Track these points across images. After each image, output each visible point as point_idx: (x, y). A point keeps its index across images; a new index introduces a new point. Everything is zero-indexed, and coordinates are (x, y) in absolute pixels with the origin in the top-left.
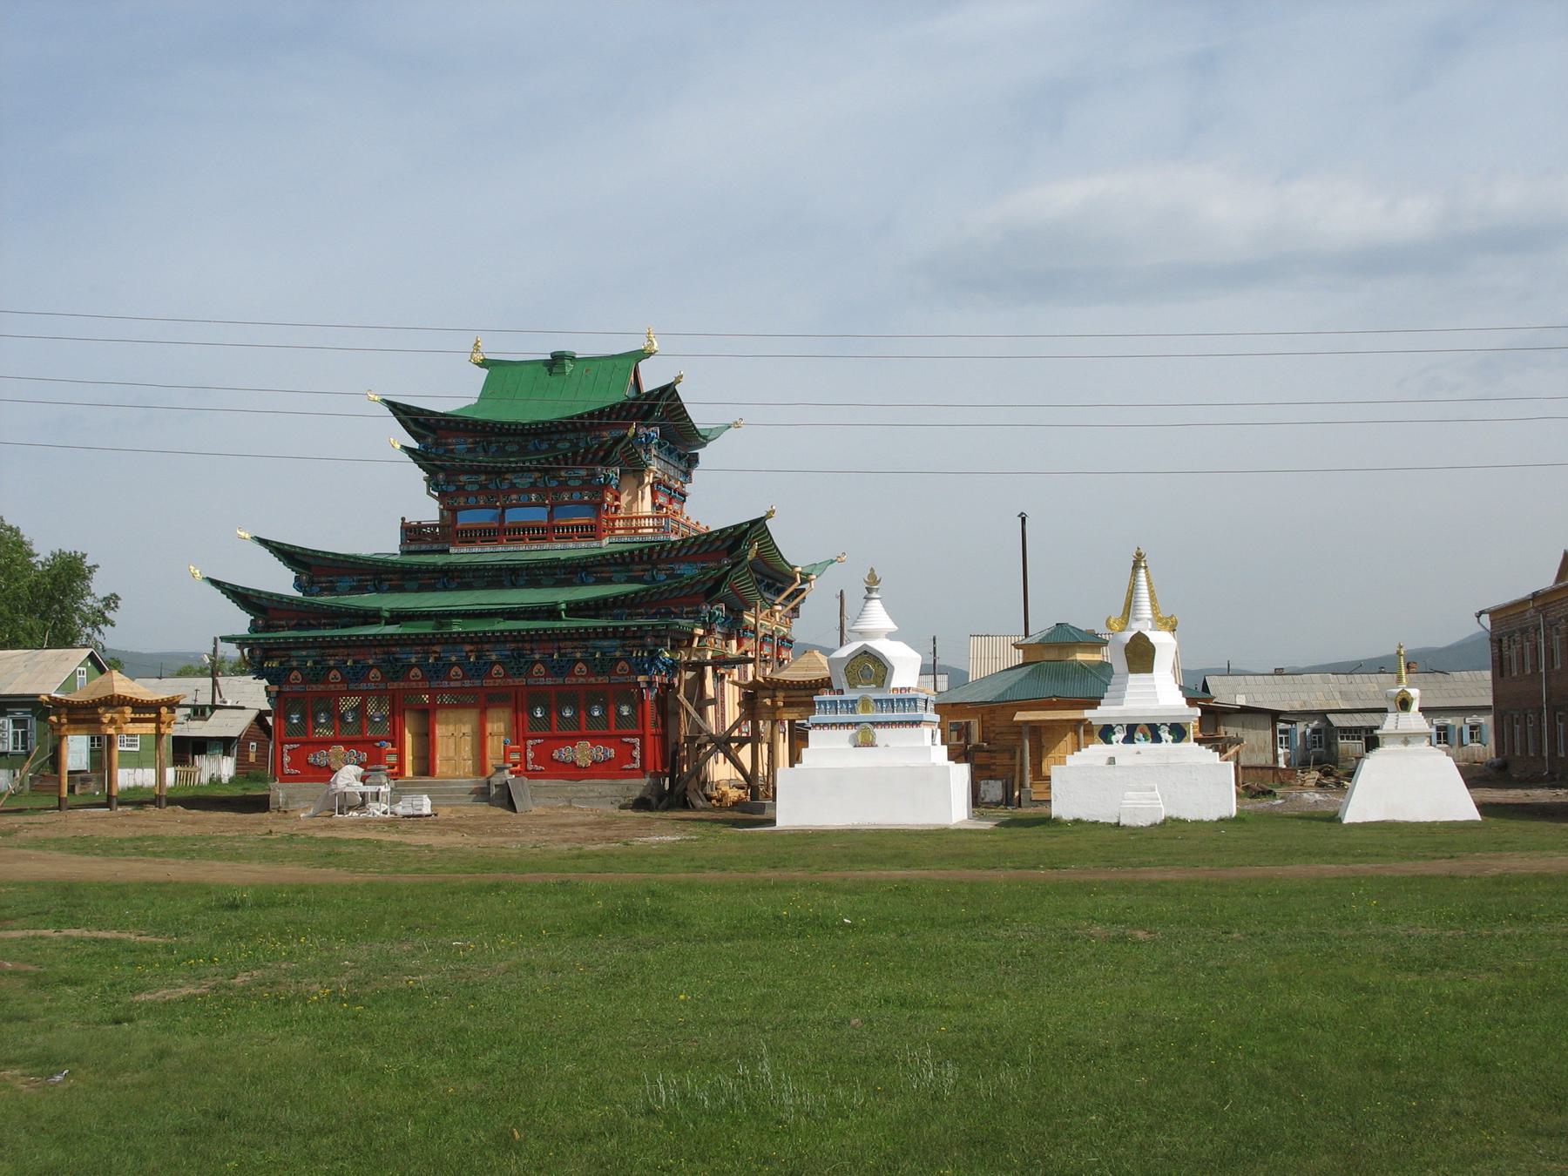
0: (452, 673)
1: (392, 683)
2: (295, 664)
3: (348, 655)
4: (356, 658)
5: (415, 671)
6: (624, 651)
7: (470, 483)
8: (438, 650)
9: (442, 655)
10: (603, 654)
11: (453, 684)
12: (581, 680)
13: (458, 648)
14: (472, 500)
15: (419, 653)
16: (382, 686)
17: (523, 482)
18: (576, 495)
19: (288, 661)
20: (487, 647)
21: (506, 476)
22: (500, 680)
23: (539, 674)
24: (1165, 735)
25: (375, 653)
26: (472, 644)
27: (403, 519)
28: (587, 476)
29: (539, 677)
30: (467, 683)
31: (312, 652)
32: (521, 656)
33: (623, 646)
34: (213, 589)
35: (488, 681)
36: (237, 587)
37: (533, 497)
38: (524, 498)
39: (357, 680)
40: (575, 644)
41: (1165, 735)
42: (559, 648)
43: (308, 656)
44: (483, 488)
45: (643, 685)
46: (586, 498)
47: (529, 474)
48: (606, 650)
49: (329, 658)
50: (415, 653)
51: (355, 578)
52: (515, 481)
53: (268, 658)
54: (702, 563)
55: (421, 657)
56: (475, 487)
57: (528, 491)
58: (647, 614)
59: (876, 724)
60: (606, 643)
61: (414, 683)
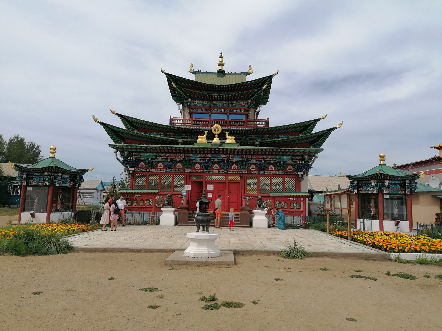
0: (214, 167)
1: (187, 170)
2: (142, 159)
4: (172, 158)
5: (198, 165)
6: (293, 161)
9: (211, 159)
10: (283, 162)
11: (215, 171)
12: (272, 172)
14: (200, 110)
15: (201, 157)
16: (182, 171)
17: (219, 104)
19: (139, 158)
20: (232, 156)
21: (213, 102)
22: (236, 171)
23: (253, 169)
26: (225, 154)
27: (171, 116)
28: (243, 104)
29: (253, 170)
30: (221, 172)
31: (152, 154)
32: (247, 161)
33: (292, 159)
34: (102, 127)
35: (230, 171)
36: (114, 127)
37: (223, 110)
38: (219, 111)
39: (171, 168)
40: (271, 157)
42: (264, 158)
43: (149, 156)
44: (204, 106)
46: (242, 112)
48: (284, 160)
49: (159, 157)
50: (199, 157)
51: (156, 134)
52: (216, 104)
53: (129, 156)
55: (202, 159)
57: (221, 108)
60: (284, 157)
61: (197, 170)
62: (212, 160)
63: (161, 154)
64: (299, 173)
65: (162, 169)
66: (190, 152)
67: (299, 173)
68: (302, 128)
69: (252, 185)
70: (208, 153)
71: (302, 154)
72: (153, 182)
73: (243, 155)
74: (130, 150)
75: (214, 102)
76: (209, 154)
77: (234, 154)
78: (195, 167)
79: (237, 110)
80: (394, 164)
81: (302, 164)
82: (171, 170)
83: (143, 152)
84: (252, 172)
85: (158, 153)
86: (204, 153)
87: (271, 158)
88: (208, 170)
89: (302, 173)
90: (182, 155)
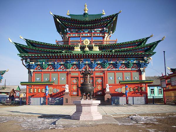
3: (55, 61)
8: (82, 60)
13: (89, 59)
16: (65, 70)
20: (97, 59)
25: (63, 61)
26: (92, 58)
27: (56, 40)
31: (44, 60)
45: (142, 71)
47: (88, 30)
63: (50, 60)
64: (141, 69)
66: (69, 57)
67: (141, 69)
68: (139, 43)
69: (111, 78)
70: (81, 58)
71: (143, 56)
72: (46, 78)
73: (105, 58)
74: (31, 58)
76: (82, 58)
77: (99, 58)
81: (143, 62)
83: (39, 59)
85: (48, 59)
86: (78, 58)
89: (143, 69)
90: (64, 60)
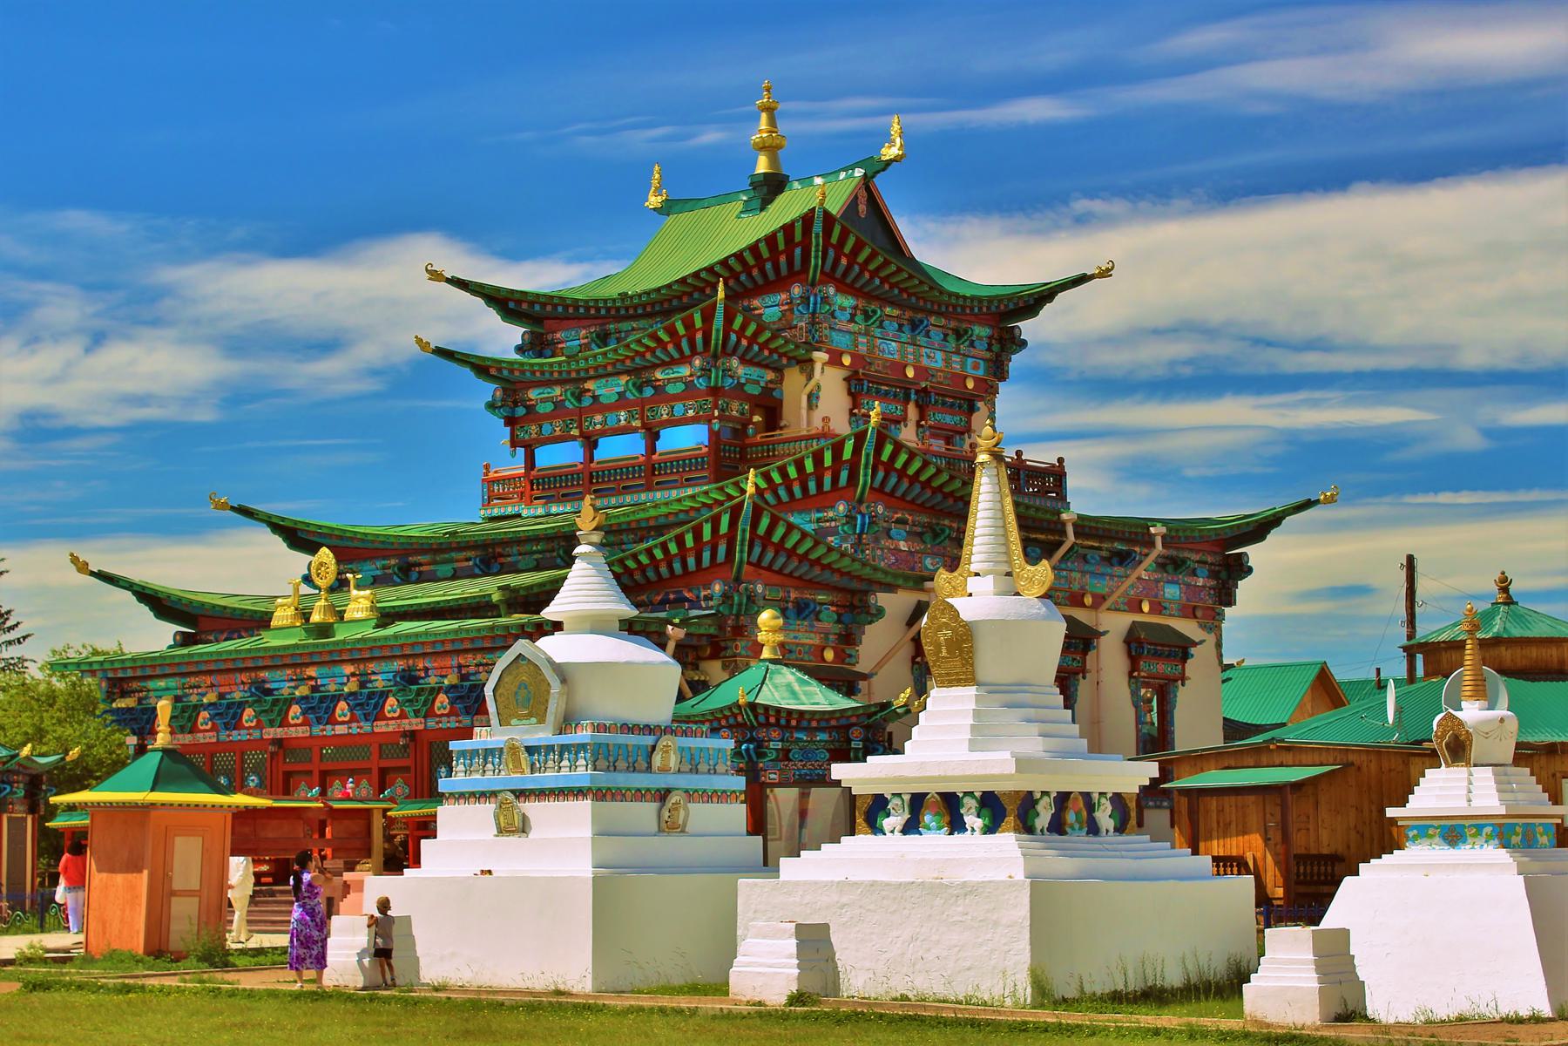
3: (212, 686)
4: (223, 690)
7: (543, 401)
14: (547, 429)
18: (679, 409)
21: (587, 385)
24: (972, 820)
41: (972, 820)
51: (379, 564)
54: (819, 511)
56: (549, 407)
58: (651, 603)
59: (521, 794)
62: (322, 689)
65: (207, 734)
75: (590, 385)
78: (290, 718)
79: (673, 408)
80: (1497, 576)
82: (229, 736)
84: (437, 723)
87: (481, 665)
88: (321, 727)
